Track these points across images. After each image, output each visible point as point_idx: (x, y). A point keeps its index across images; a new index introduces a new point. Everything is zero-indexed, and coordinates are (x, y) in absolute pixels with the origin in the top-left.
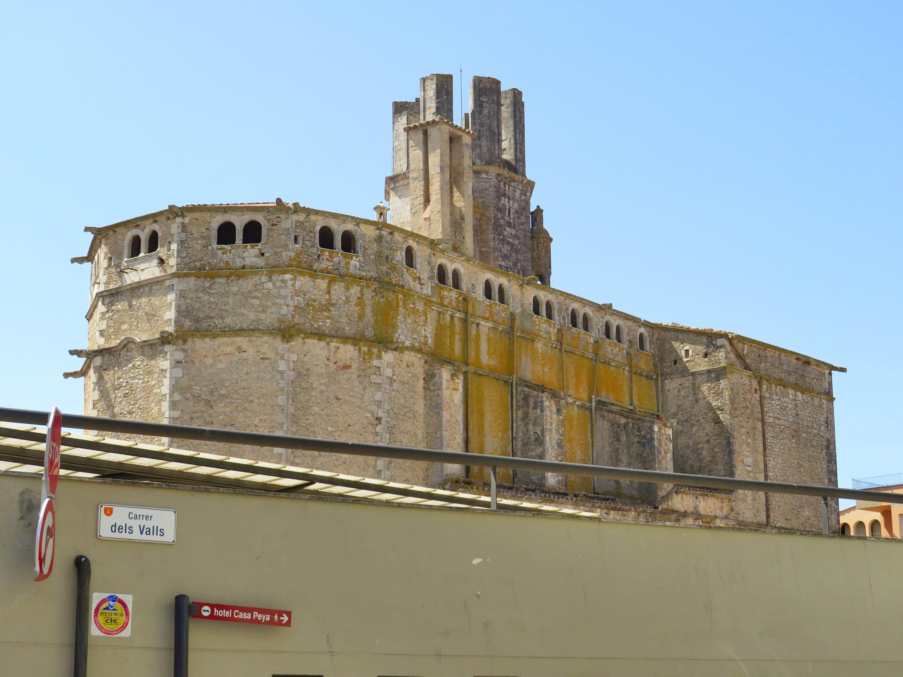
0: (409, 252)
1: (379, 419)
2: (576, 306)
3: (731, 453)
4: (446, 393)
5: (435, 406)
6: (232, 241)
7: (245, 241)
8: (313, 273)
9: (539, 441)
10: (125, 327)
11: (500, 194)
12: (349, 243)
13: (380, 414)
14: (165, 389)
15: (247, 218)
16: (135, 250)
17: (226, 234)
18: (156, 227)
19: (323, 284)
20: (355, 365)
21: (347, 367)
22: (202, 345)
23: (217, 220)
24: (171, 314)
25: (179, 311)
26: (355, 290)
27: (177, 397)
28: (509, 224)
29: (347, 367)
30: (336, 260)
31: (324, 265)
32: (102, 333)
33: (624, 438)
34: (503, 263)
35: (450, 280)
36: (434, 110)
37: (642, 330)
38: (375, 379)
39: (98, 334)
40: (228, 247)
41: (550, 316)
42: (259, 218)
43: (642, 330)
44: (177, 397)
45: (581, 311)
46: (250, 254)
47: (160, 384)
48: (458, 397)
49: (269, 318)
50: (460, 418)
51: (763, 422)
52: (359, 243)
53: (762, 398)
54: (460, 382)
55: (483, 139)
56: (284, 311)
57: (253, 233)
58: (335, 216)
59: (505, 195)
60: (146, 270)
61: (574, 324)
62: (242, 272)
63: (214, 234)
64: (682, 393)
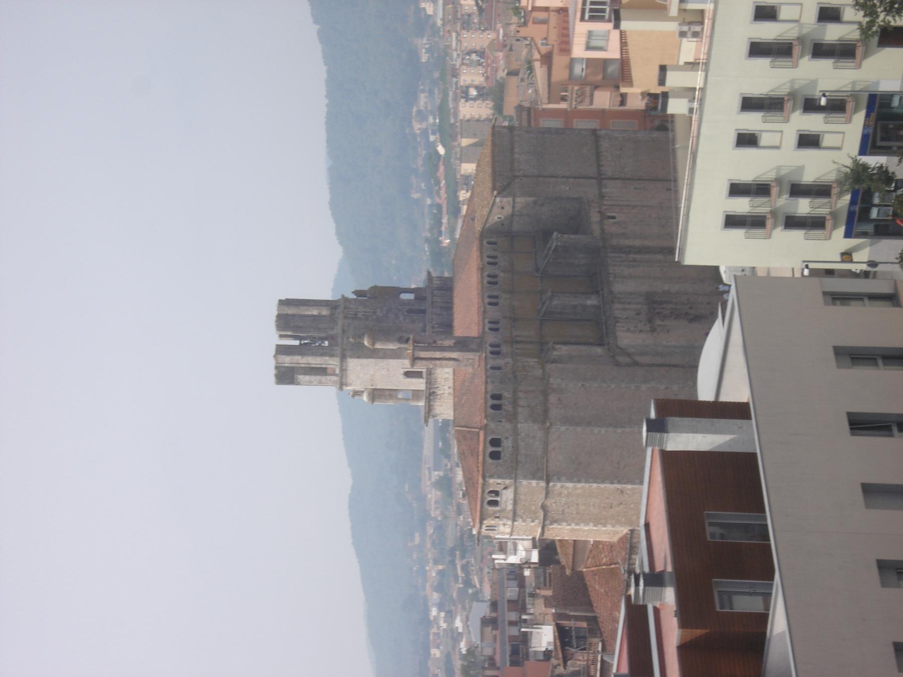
0: (493, 368)
1: (583, 385)
2: (485, 282)
6: (499, 452)
9: (575, 307)
10: (533, 508)
11: (355, 317)
12: (495, 397)
15: (488, 445)
16: (494, 503)
17: (495, 456)
18: (487, 491)
19: (520, 410)
21: (559, 399)
23: (489, 460)
24: (534, 483)
25: (533, 479)
26: (521, 395)
28: (375, 313)
32: (533, 521)
34: (402, 317)
35: (497, 349)
36: (300, 357)
39: (532, 524)
40: (502, 455)
41: (496, 297)
42: (489, 438)
43: (485, 242)
44: (575, 479)
45: (487, 279)
46: (507, 444)
47: (567, 488)
50: (574, 347)
51: (538, 176)
53: (525, 176)
54: (557, 346)
57: (495, 442)
58: (486, 403)
59: (356, 314)
60: (507, 497)
61: (495, 283)
62: (516, 448)
63: (495, 461)
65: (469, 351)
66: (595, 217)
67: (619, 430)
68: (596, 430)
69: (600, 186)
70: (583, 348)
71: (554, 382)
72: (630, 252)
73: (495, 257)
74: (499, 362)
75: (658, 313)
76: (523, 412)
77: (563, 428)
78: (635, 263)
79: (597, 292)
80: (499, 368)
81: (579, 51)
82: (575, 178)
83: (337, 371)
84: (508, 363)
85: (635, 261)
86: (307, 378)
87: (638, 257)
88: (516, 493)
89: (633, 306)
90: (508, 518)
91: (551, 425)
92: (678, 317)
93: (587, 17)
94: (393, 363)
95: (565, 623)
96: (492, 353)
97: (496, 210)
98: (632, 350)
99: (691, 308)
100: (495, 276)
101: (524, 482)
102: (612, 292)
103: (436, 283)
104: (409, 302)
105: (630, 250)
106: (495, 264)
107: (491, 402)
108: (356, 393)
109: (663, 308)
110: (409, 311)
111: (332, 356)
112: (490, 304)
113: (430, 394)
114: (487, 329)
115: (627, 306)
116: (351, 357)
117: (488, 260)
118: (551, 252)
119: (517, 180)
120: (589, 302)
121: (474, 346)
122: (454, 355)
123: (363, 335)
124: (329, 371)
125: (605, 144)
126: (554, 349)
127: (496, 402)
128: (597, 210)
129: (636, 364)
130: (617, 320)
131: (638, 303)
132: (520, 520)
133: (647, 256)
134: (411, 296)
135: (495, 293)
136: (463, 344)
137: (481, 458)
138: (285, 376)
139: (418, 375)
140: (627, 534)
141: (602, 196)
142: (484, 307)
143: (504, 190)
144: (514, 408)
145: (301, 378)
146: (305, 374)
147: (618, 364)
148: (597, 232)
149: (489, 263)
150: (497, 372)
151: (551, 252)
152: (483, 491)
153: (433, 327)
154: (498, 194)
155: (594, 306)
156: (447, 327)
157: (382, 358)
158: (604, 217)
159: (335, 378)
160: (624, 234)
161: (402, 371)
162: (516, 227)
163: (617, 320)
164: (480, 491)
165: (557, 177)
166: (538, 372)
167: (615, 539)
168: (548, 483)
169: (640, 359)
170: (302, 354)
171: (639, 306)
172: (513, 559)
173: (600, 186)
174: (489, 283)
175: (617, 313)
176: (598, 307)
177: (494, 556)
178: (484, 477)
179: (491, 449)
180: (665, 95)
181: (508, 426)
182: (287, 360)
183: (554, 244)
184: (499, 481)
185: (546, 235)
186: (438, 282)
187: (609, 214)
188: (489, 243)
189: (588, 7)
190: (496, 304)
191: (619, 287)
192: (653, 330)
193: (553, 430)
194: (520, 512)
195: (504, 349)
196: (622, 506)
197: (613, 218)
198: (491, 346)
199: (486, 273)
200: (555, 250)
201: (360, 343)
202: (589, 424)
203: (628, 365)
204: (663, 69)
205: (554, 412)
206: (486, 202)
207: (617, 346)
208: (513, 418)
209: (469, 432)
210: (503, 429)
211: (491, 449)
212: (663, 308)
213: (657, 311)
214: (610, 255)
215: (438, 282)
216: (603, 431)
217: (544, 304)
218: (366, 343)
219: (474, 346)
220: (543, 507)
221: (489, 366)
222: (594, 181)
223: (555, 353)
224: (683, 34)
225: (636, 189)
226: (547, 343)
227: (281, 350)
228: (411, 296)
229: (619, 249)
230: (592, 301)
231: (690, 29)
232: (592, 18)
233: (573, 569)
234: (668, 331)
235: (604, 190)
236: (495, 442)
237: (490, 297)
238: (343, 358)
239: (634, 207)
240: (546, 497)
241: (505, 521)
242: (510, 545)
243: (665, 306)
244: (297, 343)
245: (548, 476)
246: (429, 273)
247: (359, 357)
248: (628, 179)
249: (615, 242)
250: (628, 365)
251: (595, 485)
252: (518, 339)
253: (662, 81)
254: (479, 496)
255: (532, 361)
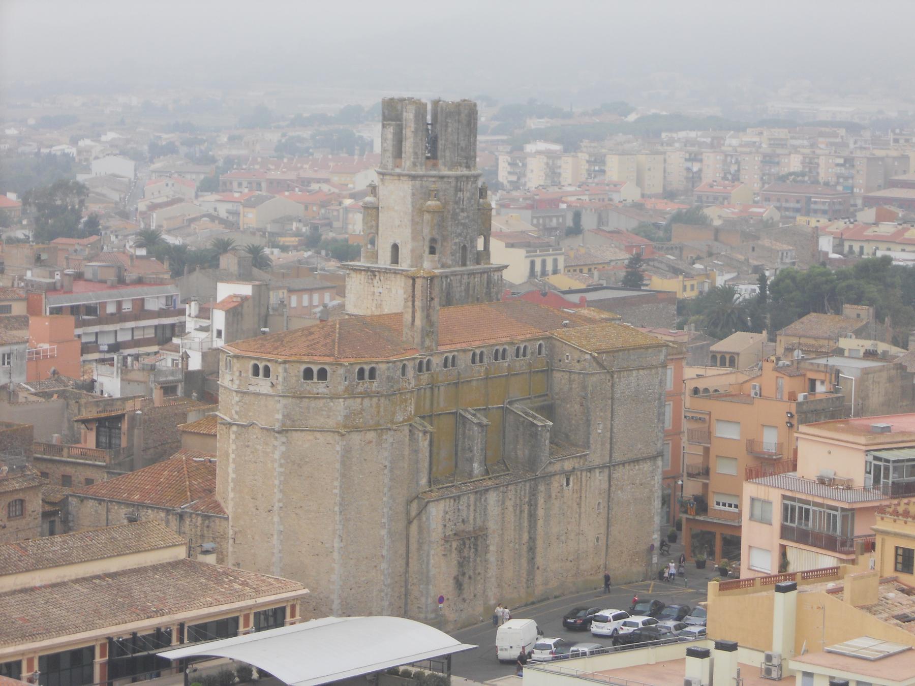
0: (404, 366)
2: (498, 347)
3: (589, 426)
4: (421, 444)
5: (416, 451)
7: (318, 379)
8: (353, 396)
11: (458, 189)
13: (387, 463)
14: (277, 455)
15: (320, 367)
16: (256, 372)
17: (308, 374)
18: (269, 364)
19: (359, 400)
20: (374, 440)
21: (370, 442)
22: (294, 434)
23: (303, 367)
24: (280, 416)
25: (283, 416)
26: (375, 400)
27: (283, 461)
28: (463, 210)
29: (370, 442)
30: (365, 385)
31: (360, 389)
32: (237, 412)
33: (521, 429)
34: (457, 241)
35: (424, 368)
37: (541, 342)
38: (384, 445)
39: (233, 412)
41: (481, 361)
42: (327, 367)
44: (283, 461)
46: (321, 388)
47: (273, 453)
48: (427, 443)
49: (331, 423)
50: (427, 454)
51: (612, 399)
52: (377, 373)
53: (613, 385)
55: (447, 151)
56: (339, 418)
58: (366, 363)
60: (262, 385)
61: (496, 359)
63: (302, 374)
64: (563, 381)
65: (422, 337)
66: (568, 465)
67: (337, 509)
68: (337, 483)
69: (602, 467)
70: (426, 465)
71: (389, 437)
72: (530, 505)
73: (524, 355)
74: (410, 373)
75: (464, 544)
76: (356, 404)
77: (338, 448)
78: (518, 512)
79: (487, 472)
80: (403, 374)
81: (750, 490)
82: (611, 439)
83: (398, 170)
84: (409, 383)
85: (521, 512)
86: (390, 136)
87: (526, 515)
88: (266, 395)
89: (471, 518)
90: (239, 386)
91: (343, 435)
92: (460, 565)
93: (786, 502)
94: (407, 232)
95: (125, 426)
96: (421, 363)
97: (576, 355)
98: (424, 519)
99: (470, 578)
100: (503, 358)
101: (279, 406)
102: (487, 490)
103: (495, 276)
104: (474, 247)
105: (533, 505)
106: (517, 356)
107: (367, 368)
108: (373, 189)
109: (470, 547)
110: (464, 248)
111: (414, 164)
112: (474, 355)
113: (373, 272)
114: (446, 355)
115: (472, 508)
116: (413, 186)
117: (522, 346)
118: (531, 419)
119: (608, 377)
120: (476, 465)
121: (428, 343)
122: (418, 322)
123: (438, 200)
124: (398, 160)
125: (646, 466)
126: (425, 432)
127: (367, 374)
128: (577, 466)
129: (410, 522)
130: (457, 498)
131: (475, 519)
132: (237, 399)
133: (526, 524)
134: (480, 246)
135: (485, 360)
136: (430, 329)
137: (305, 359)
138: (392, 112)
139: (395, 260)
140: (225, 513)
141: (590, 470)
142: (470, 350)
143: (598, 363)
144: (361, 393)
145: (390, 131)
146: (395, 134)
147: (409, 502)
148: (551, 469)
149: (518, 349)
150: (399, 372)
151: (531, 419)
152: (269, 361)
153: (447, 277)
154: (594, 357)
155: (471, 471)
156: (448, 301)
157: (413, 220)
158: (568, 475)
159: (390, 165)
160: (550, 497)
161: (398, 241)
162: (557, 375)
163: (457, 498)
164: (269, 357)
165: (612, 420)
166: (400, 418)
167: (218, 497)
168: (279, 432)
169: (414, 528)
170: (416, 132)
171: (472, 521)
172: (191, 325)
173: (602, 467)
174: (497, 351)
175: (464, 500)
176: (470, 475)
177: (193, 303)
178: (285, 362)
179: (315, 369)
180: (704, 654)
181: (341, 388)
182: (409, 115)
183: (540, 424)
184: (280, 379)
185: (549, 411)
186: (496, 277)
187: (571, 479)
188: (540, 346)
189: (797, 505)
190: (473, 362)
191: (492, 498)
192: (446, 539)
193: (337, 437)
194: (247, 399)
195: (425, 377)
196: (254, 510)
197: (568, 484)
198: (429, 362)
199: (507, 347)
200: (533, 424)
201: (430, 195)
202: (343, 476)
203: (408, 513)
204: (732, 647)
205: (356, 438)
206: (584, 343)
207: (428, 502)
208: (351, 394)
209: (334, 341)
210: (338, 380)
211: (315, 369)
212: (470, 547)
213: (467, 542)
214: (528, 485)
215: (496, 277)
216: (337, 491)
217: (474, 415)
218: (429, 203)
219: (428, 343)
220: (252, 424)
221: (406, 362)
222: (608, 459)
223: (421, 435)
224: (769, 658)
225: (599, 503)
226: (431, 424)
227: (420, 109)
228: (480, 246)
229: (533, 494)
230: (477, 468)
231: (774, 666)
232: (786, 508)
233: (184, 432)
234: (444, 555)
235: (597, 471)
236: (323, 374)
237: (482, 353)
238: (414, 178)
239: (579, 504)
240: (262, 429)
241: (237, 382)
242: (204, 323)
243: (473, 550)
244: (429, 119)
245: (287, 431)
246: (506, 267)
247: (413, 194)
248: (609, 496)
249: (542, 488)
250: (408, 513)
251: (277, 482)
252: (436, 390)
253: (721, 646)
254: (264, 356)
255: (411, 409)
